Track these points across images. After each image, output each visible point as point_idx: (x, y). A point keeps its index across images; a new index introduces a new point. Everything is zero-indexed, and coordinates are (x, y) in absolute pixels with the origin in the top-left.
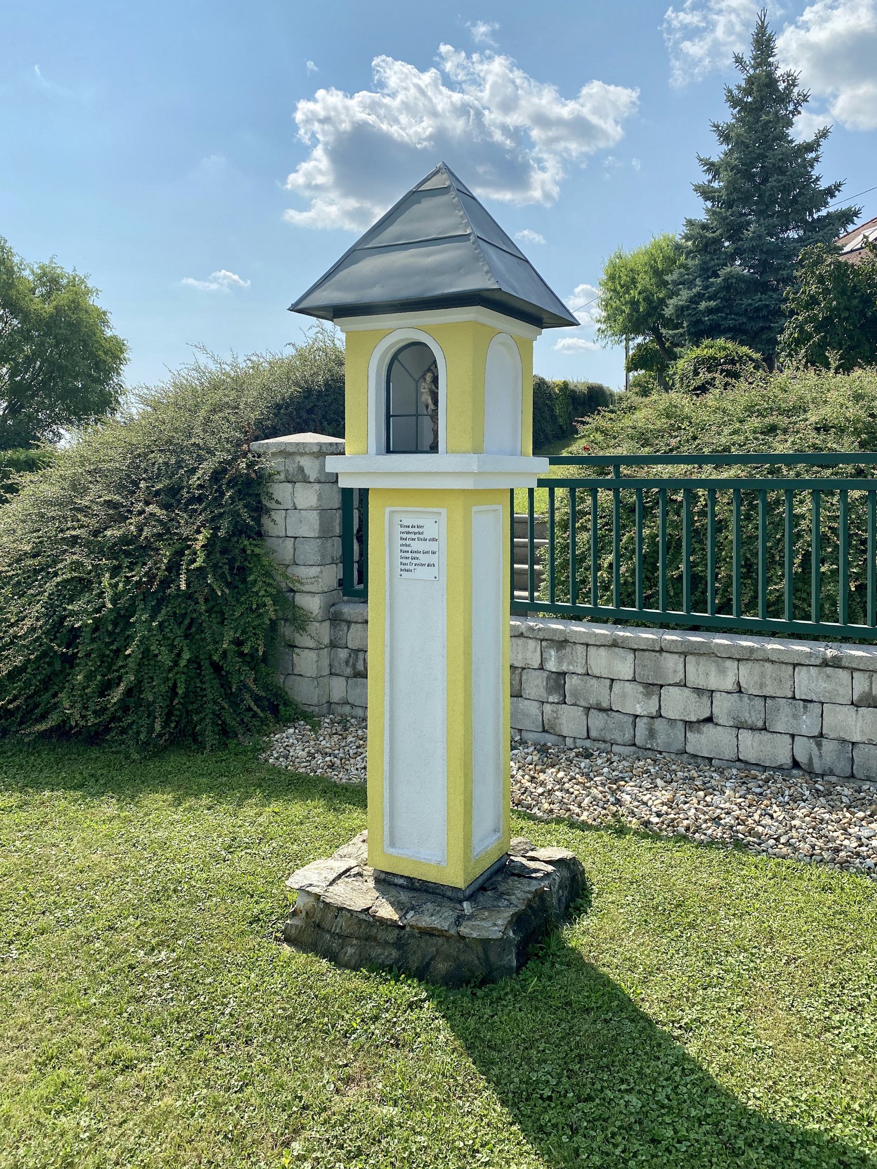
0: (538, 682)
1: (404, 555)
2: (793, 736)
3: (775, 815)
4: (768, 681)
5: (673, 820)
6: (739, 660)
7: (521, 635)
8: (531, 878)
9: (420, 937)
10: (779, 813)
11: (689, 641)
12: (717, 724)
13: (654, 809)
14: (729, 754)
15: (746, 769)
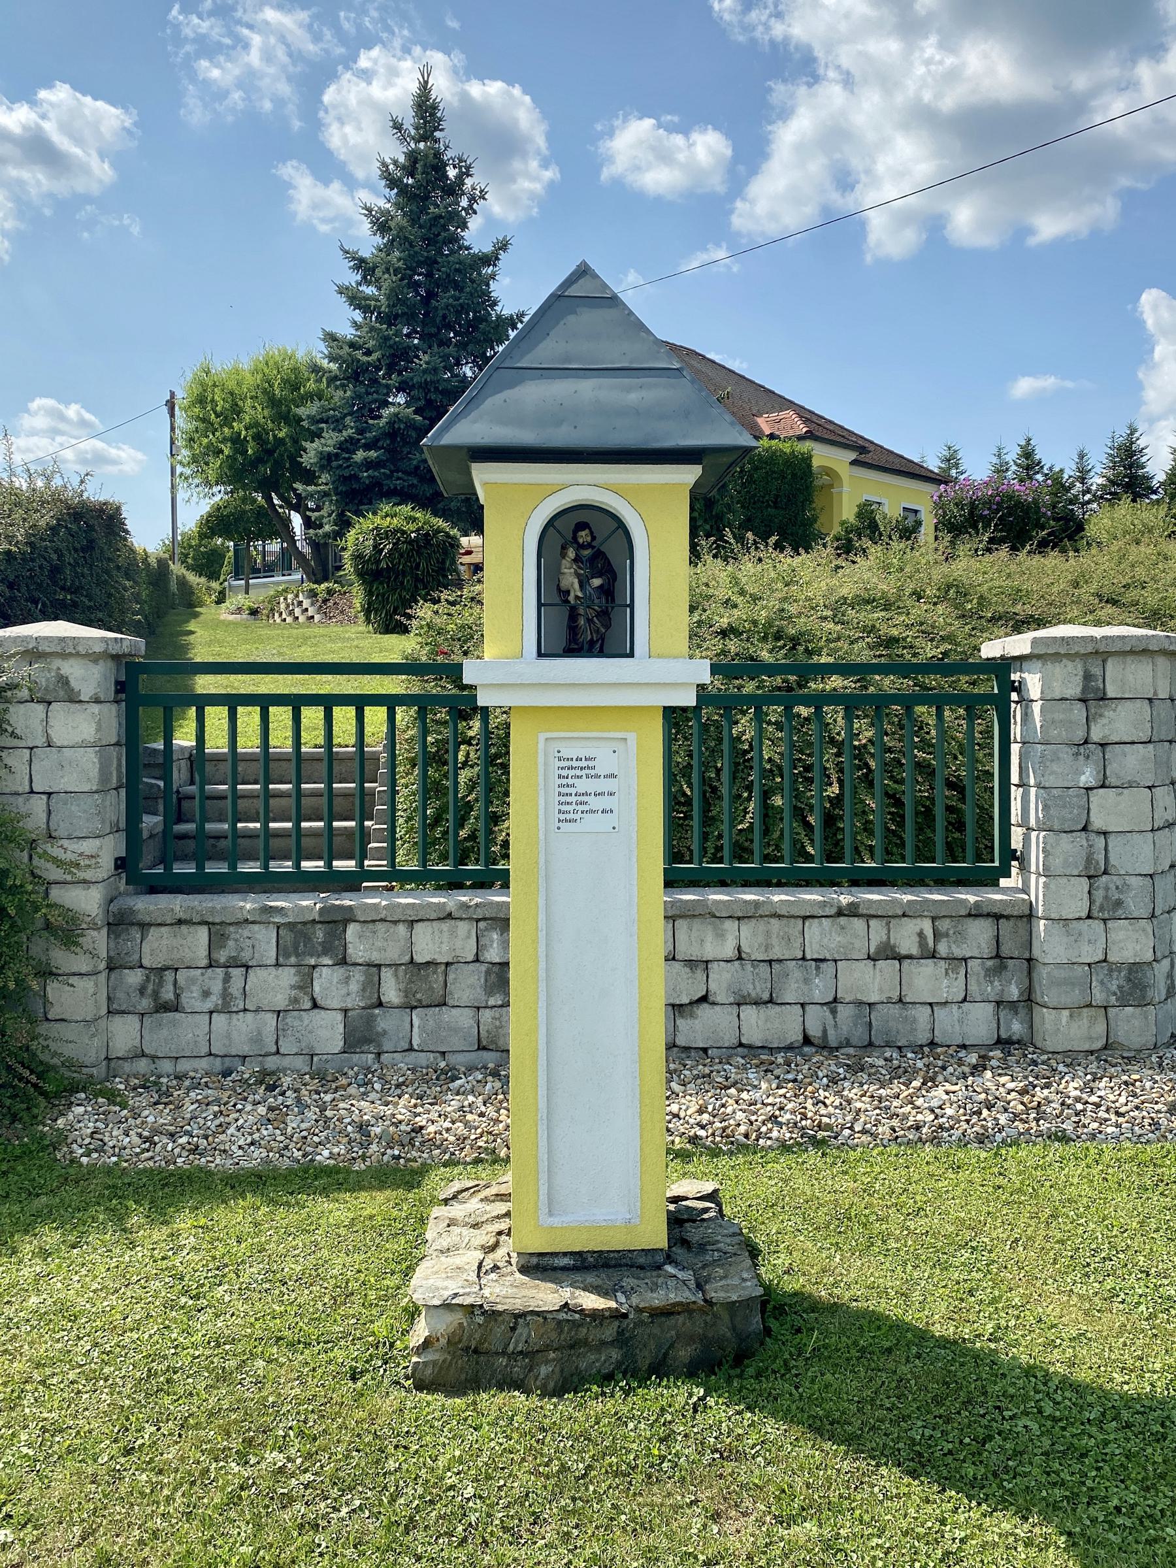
0: (472, 980)
1: (563, 799)
2: (803, 1005)
3: (828, 1102)
4: (774, 941)
5: (724, 1129)
6: (739, 919)
7: (449, 916)
8: (703, 1220)
9: (652, 1322)
10: (832, 1099)
11: (681, 901)
12: (714, 1003)
13: (692, 1121)
14: (730, 1039)
15: (758, 1055)
